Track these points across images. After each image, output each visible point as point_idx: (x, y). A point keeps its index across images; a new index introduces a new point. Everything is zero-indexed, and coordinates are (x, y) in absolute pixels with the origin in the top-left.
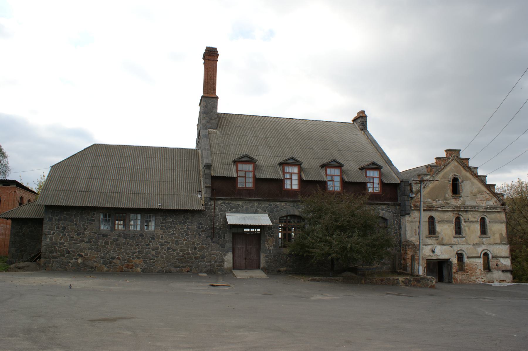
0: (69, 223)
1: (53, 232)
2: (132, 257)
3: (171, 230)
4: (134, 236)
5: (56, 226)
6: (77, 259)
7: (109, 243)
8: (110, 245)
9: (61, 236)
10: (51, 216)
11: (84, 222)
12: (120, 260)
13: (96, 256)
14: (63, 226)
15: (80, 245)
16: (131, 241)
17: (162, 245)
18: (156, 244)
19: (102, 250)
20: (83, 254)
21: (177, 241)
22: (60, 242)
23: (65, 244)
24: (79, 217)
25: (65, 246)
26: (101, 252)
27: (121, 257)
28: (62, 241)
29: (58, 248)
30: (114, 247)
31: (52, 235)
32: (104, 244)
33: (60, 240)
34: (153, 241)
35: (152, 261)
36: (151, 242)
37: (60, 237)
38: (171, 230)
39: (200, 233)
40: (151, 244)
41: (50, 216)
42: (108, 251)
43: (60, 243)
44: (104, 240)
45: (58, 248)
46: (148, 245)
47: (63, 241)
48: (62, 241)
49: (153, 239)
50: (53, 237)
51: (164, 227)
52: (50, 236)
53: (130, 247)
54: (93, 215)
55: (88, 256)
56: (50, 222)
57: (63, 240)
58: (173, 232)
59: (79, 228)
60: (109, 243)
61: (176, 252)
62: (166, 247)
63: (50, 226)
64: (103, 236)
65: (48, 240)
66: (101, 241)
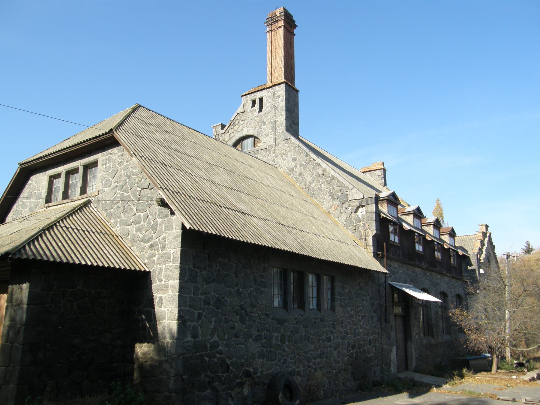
0: (228, 289)
1: (199, 313)
2: (314, 367)
3: (349, 309)
4: (315, 322)
5: (203, 297)
6: (241, 385)
7: (287, 338)
8: (287, 343)
9: (213, 323)
10: (194, 267)
11: (251, 289)
12: (301, 376)
13: (269, 372)
14: (216, 295)
15: (243, 346)
16: (312, 331)
17: (343, 338)
18: (337, 337)
19: (278, 358)
20: (252, 370)
21: (355, 330)
22: (212, 341)
23: (220, 348)
24: (242, 274)
25: (220, 353)
26: (276, 362)
27: (301, 369)
28: (214, 339)
29: (207, 359)
30: (292, 348)
31: (195, 323)
32: (279, 343)
33: (212, 335)
34: (334, 331)
35: (334, 371)
36: (332, 333)
37: (212, 327)
38: (349, 309)
39: (373, 314)
40: (332, 336)
41: (191, 267)
42: (285, 358)
43: (211, 343)
44: (279, 332)
45: (207, 359)
46: (329, 340)
47: (217, 340)
48: (216, 338)
49: (334, 326)
50: (199, 328)
51: (343, 303)
52: (192, 324)
53: (311, 345)
54: (264, 272)
55: (258, 375)
56: (193, 285)
57: (218, 336)
58: (351, 313)
59: (243, 303)
60: (287, 338)
61: (355, 350)
62: (347, 342)
63: (192, 296)
64: (278, 323)
65: (189, 338)
66: (275, 334)
